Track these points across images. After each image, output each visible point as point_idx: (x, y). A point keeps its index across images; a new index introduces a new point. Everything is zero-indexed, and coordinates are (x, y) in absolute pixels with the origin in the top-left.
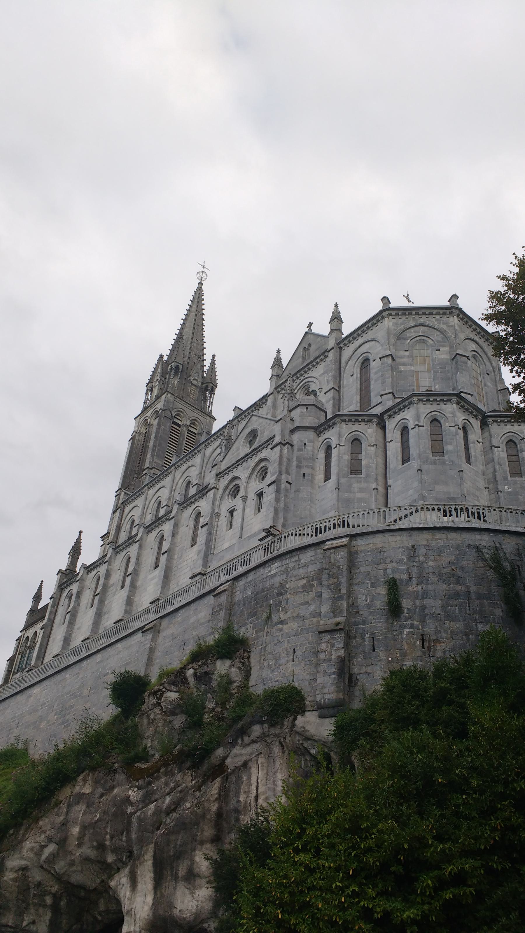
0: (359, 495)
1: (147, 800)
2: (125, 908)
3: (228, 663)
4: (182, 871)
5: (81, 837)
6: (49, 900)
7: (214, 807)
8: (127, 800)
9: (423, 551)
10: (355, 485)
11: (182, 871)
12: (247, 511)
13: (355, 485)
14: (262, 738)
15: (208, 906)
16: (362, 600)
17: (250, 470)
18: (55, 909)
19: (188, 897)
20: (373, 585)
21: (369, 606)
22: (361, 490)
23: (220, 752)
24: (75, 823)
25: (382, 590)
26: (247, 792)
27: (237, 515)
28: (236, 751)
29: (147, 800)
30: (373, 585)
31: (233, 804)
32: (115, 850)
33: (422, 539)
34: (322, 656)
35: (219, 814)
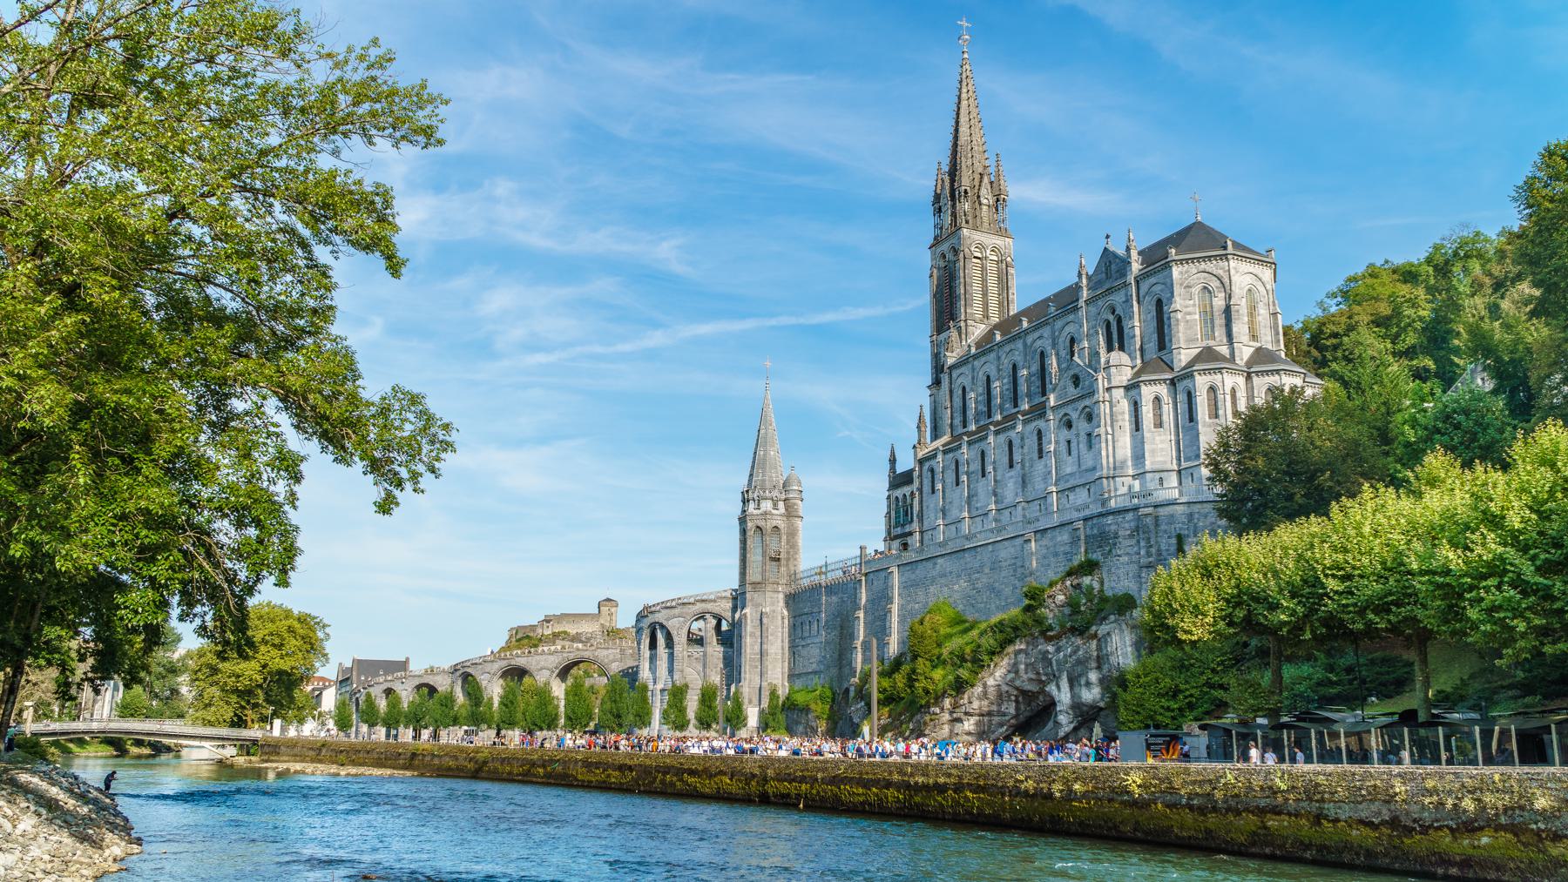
0: (1160, 446)
1: (1058, 650)
2: (1057, 699)
3: (1090, 578)
4: (1083, 682)
5: (1026, 670)
6: (1013, 698)
7: (1095, 654)
8: (1048, 652)
9: (1196, 516)
10: (1157, 438)
11: (1083, 682)
12: (1081, 446)
13: (1157, 438)
14: (1115, 621)
15: (1099, 696)
16: (1163, 547)
17: (1078, 412)
18: (1017, 702)
19: (1088, 693)
20: (1169, 537)
21: (1167, 550)
22: (1162, 442)
23: (1094, 628)
24: (1021, 663)
25: (1174, 541)
26: (1112, 647)
27: (1073, 445)
28: (1103, 627)
29: (1058, 650)
30: (1169, 537)
31: (1105, 652)
32: (1046, 675)
33: (1196, 508)
34: (1143, 580)
35: (1098, 657)
